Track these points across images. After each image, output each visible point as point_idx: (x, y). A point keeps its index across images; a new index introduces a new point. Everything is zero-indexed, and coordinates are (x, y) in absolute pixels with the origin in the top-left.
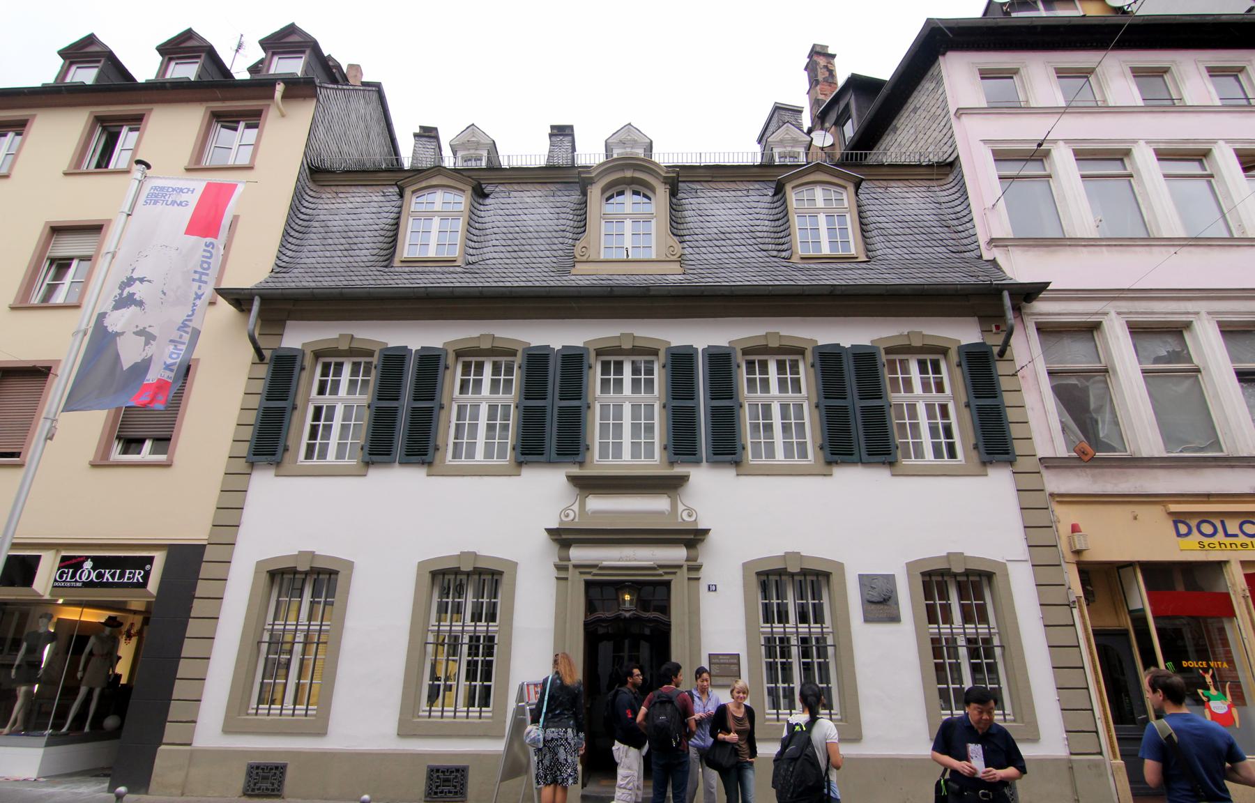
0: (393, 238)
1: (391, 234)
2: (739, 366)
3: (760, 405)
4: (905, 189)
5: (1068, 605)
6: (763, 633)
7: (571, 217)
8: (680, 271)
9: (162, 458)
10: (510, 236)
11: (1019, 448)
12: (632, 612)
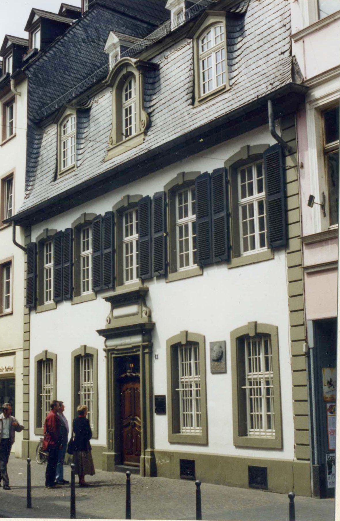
11: (293, 231)
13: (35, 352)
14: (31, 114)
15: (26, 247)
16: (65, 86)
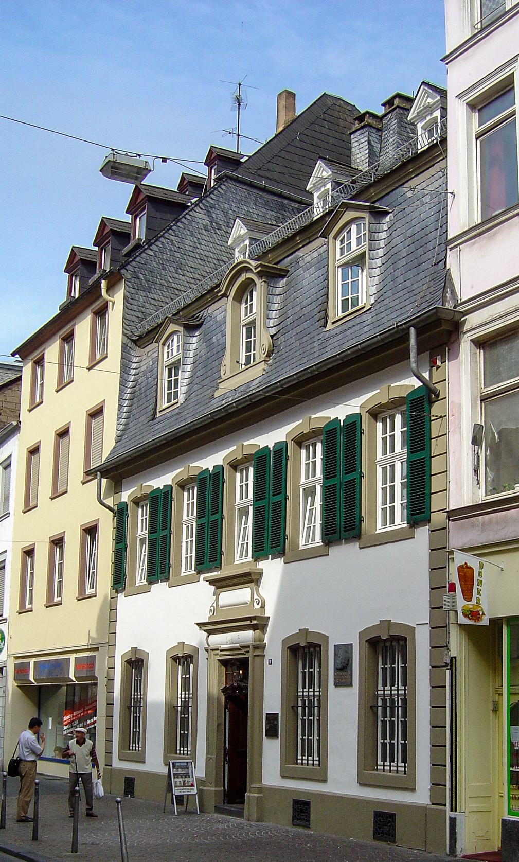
13: (122, 648)
14: (128, 328)
15: (116, 508)
16: (177, 289)
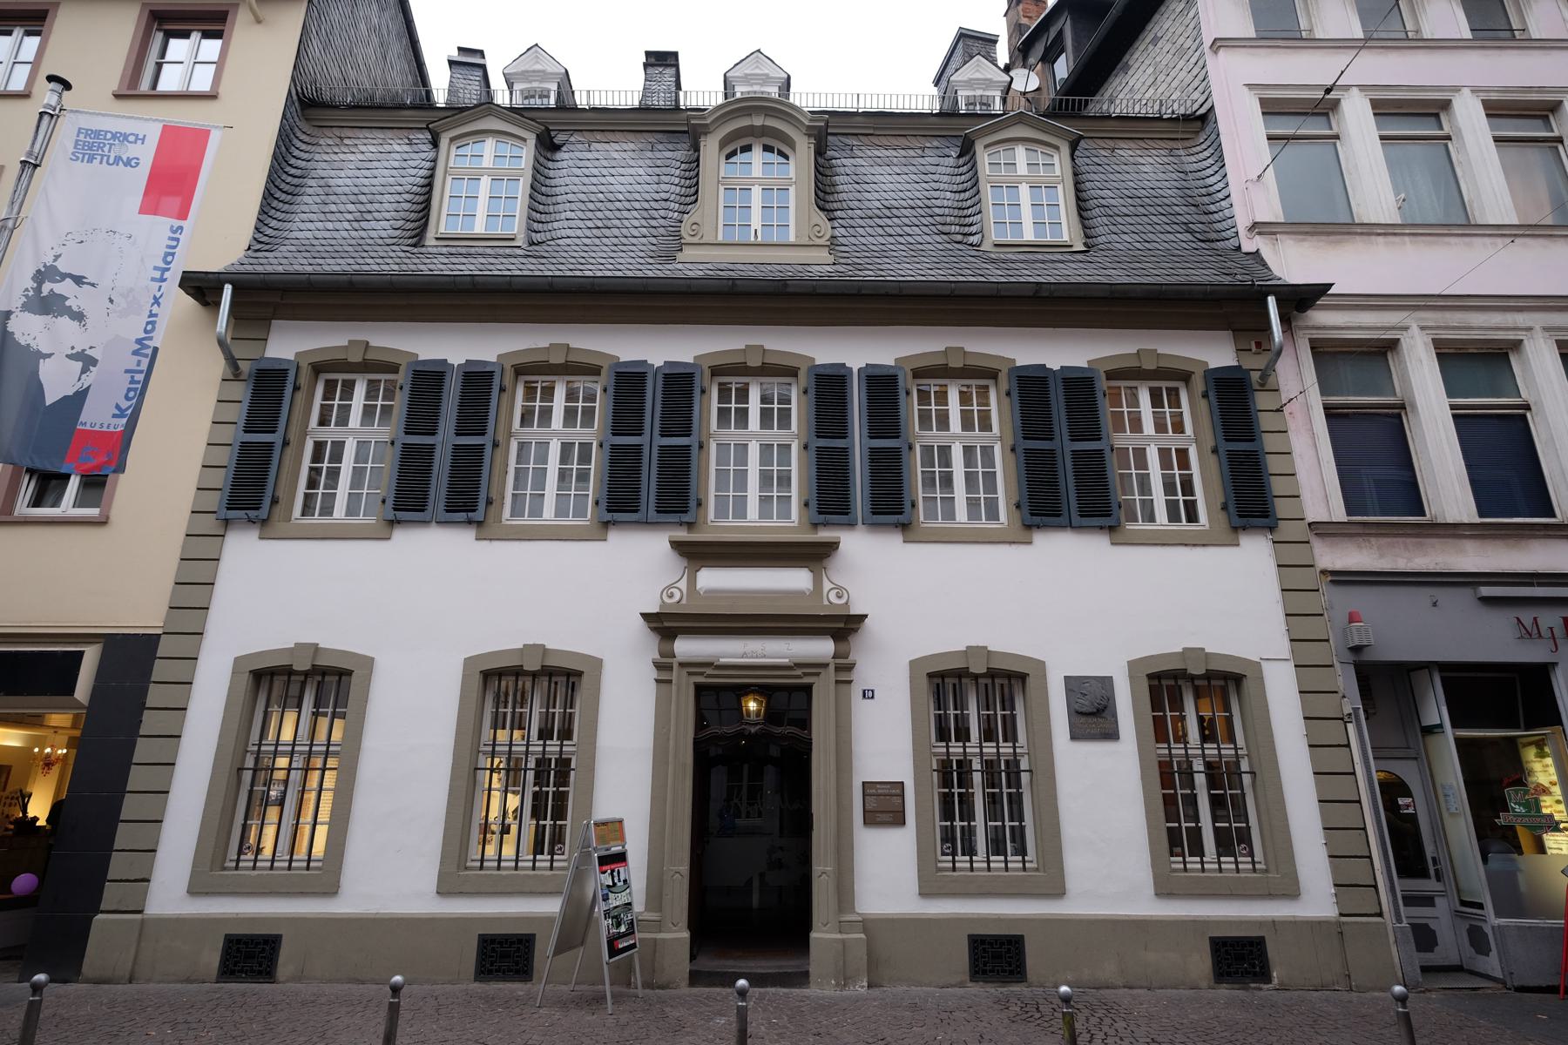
0: (423, 205)
1: (422, 198)
2: (908, 393)
3: (936, 447)
4: (1138, 152)
5: (1342, 719)
6: (935, 754)
7: (677, 181)
8: (831, 259)
9: (93, 512)
10: (591, 206)
11: (1282, 508)
12: (758, 727)
